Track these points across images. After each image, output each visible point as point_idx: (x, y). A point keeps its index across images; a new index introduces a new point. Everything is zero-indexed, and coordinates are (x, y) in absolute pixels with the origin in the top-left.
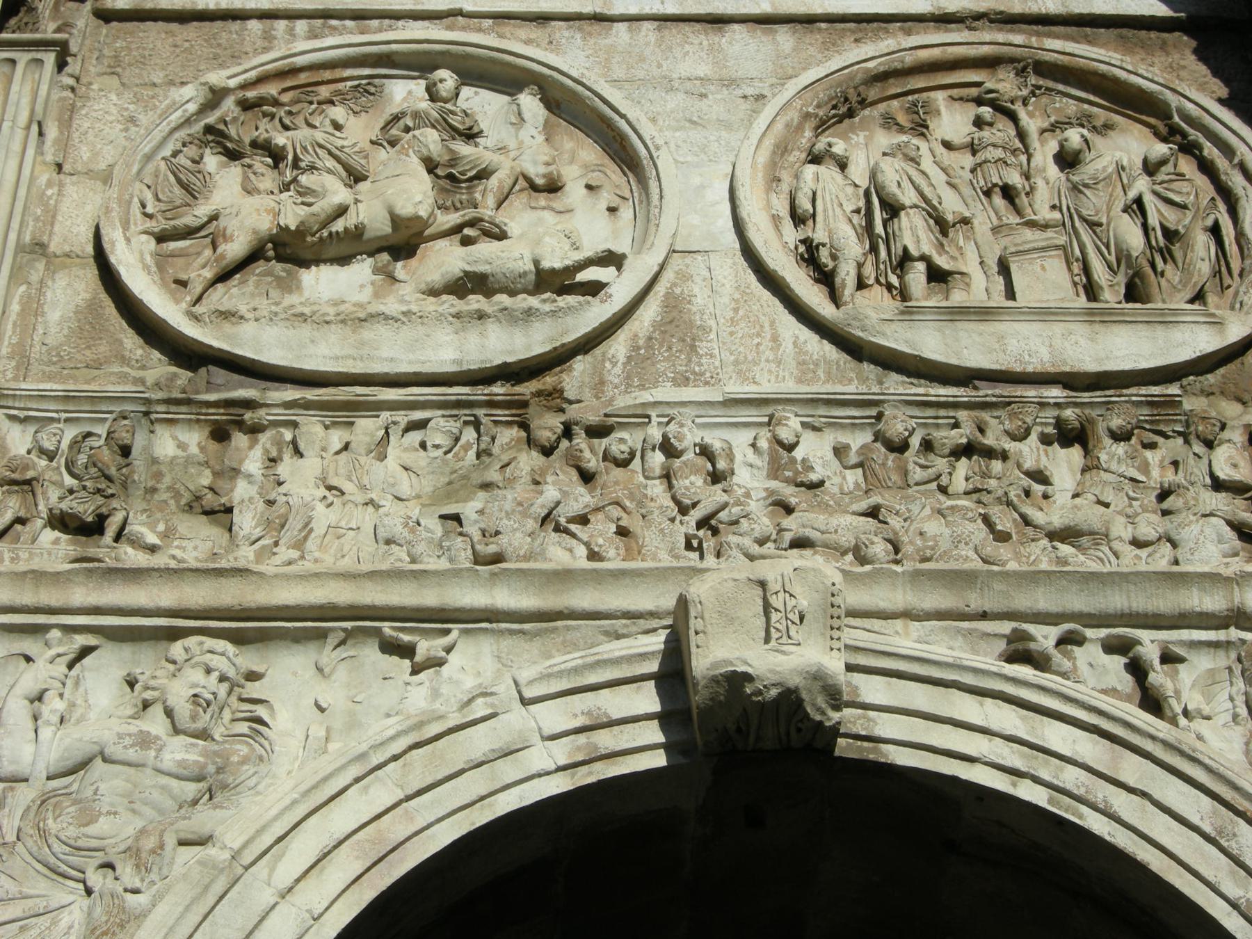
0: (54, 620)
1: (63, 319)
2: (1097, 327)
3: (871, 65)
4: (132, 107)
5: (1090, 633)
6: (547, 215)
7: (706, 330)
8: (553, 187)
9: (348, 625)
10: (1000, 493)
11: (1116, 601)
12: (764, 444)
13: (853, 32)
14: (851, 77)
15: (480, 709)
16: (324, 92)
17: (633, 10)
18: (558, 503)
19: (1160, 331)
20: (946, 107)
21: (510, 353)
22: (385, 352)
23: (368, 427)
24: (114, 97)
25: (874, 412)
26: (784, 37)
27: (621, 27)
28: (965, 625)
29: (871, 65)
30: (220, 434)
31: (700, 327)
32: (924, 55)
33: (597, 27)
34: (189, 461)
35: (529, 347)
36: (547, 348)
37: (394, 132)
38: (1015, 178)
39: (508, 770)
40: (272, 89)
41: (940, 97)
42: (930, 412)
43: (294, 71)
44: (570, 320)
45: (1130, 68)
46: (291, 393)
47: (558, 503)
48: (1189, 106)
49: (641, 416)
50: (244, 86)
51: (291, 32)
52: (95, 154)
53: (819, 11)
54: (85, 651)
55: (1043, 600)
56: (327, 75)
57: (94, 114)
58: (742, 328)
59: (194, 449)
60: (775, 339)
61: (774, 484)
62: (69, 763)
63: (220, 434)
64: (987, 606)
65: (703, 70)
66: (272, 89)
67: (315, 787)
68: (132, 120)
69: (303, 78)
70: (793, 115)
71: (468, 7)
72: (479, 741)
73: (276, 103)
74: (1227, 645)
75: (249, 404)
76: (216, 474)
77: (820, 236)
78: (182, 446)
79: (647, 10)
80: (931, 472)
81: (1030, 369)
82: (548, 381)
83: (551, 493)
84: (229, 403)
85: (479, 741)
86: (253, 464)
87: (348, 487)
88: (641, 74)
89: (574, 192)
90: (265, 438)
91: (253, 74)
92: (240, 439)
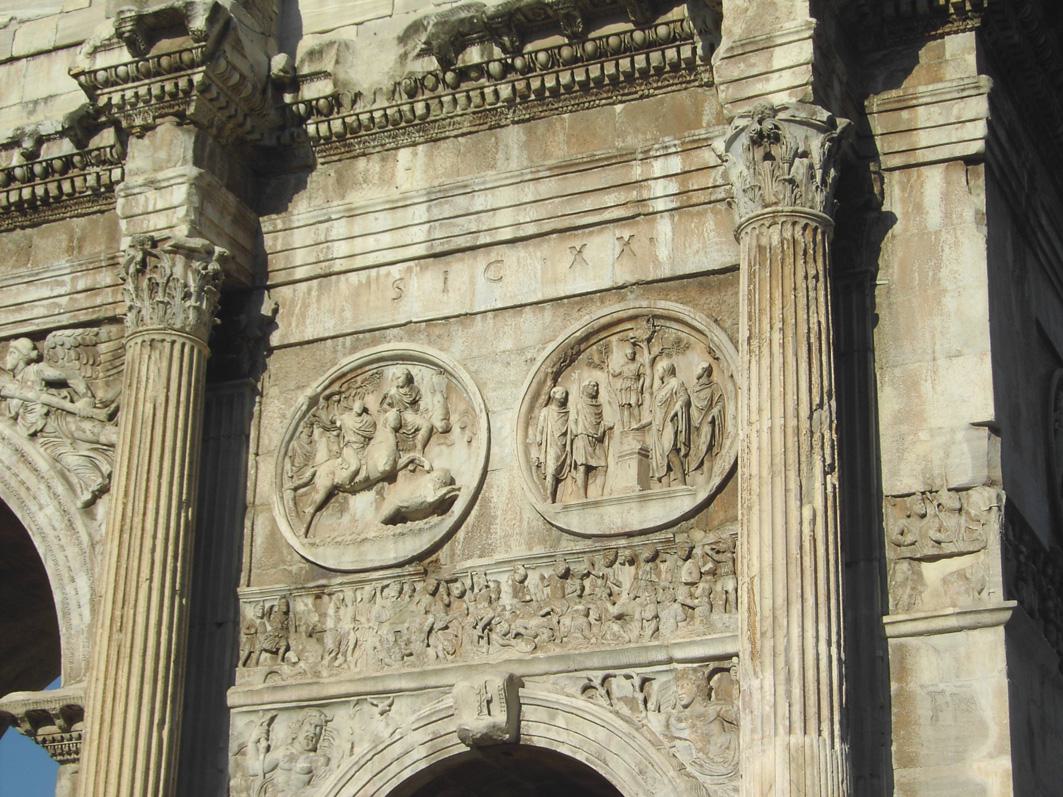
0: (260, 708)
1: (262, 543)
2: (643, 503)
3: (577, 334)
4: (283, 406)
5: (617, 672)
6: (444, 447)
7: (495, 517)
8: (447, 431)
9: (356, 698)
10: (599, 595)
11: (624, 660)
12: (510, 582)
13: (577, 303)
14: (568, 344)
15: (397, 736)
16: (359, 379)
17: (483, 309)
18: (433, 624)
19: (668, 502)
20: (617, 346)
21: (415, 551)
22: (369, 557)
23: (368, 588)
24: (276, 402)
25: (553, 559)
26: (548, 311)
27: (479, 317)
28: (571, 674)
29: (577, 334)
30: (318, 597)
31: (492, 517)
32: (603, 321)
33: (468, 321)
34: (309, 612)
35: (421, 547)
36: (429, 546)
37: (385, 406)
38: (633, 402)
39: (407, 760)
40: (335, 387)
41: (614, 339)
42: (576, 556)
43: (344, 375)
44: (437, 530)
45: (692, 315)
46: (339, 579)
47: (433, 624)
48: (715, 338)
49: (465, 571)
50: (325, 389)
51: (344, 344)
52: (270, 440)
53: (563, 295)
54: (272, 719)
55: (596, 662)
56: (359, 371)
57: (270, 414)
58: (509, 517)
59: (310, 606)
60: (521, 520)
61: (515, 601)
62: (271, 768)
63: (318, 597)
64: (576, 668)
65: (507, 344)
66: (335, 387)
67: (341, 778)
68: (284, 416)
69: (349, 376)
70: (541, 375)
71: (414, 320)
72: (397, 749)
73: (339, 393)
74: (671, 671)
75: (324, 586)
76: (320, 615)
77: (542, 460)
78: (306, 605)
79: (489, 308)
80: (574, 588)
81: (613, 532)
82: (434, 557)
83: (430, 619)
84: (318, 587)
85: (397, 749)
86: (331, 611)
87: (363, 620)
88: (484, 352)
89: (456, 430)
90: (334, 597)
91: (327, 382)
92: (326, 598)
